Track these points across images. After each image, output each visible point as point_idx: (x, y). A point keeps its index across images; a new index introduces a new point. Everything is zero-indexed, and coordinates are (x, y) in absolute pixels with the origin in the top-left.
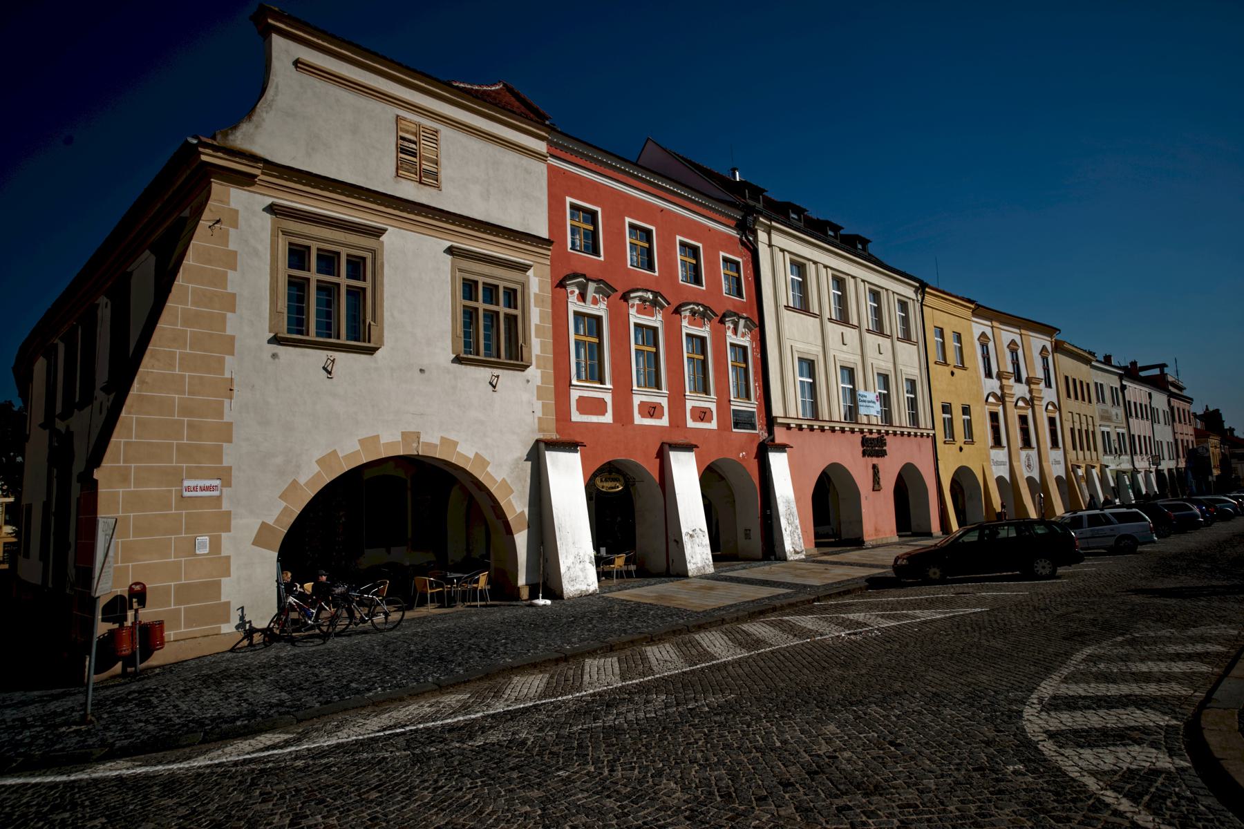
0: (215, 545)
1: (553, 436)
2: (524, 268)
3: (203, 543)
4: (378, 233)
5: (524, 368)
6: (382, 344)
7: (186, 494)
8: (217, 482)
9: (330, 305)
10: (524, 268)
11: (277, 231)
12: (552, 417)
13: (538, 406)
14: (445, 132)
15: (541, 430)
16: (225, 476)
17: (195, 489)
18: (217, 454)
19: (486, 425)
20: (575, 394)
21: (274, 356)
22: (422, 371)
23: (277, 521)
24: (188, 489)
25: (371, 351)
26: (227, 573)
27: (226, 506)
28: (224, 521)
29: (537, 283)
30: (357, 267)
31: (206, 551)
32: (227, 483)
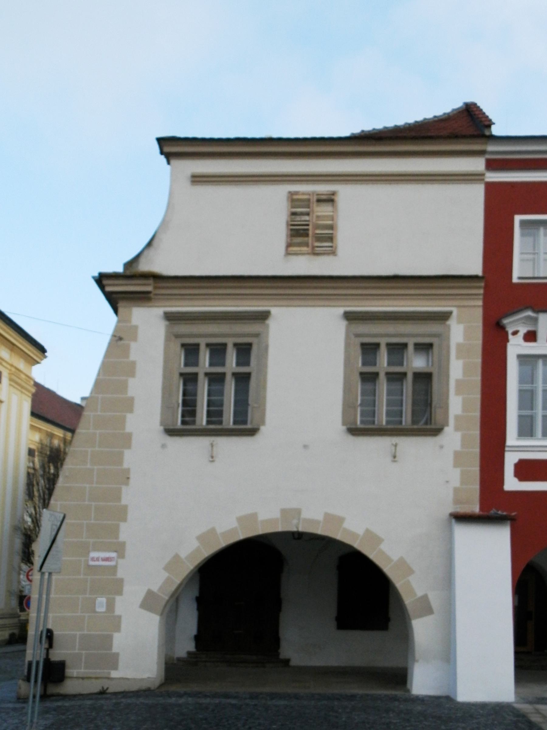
0: (111, 605)
1: (476, 509)
2: (444, 317)
3: (101, 603)
4: (264, 316)
5: (436, 431)
6: (263, 422)
7: (91, 563)
8: (113, 555)
9: (216, 394)
10: (444, 317)
11: (171, 336)
12: (475, 487)
13: (455, 477)
14: (345, 193)
15: (457, 501)
16: (120, 549)
17: (98, 559)
18: (115, 531)
19: (397, 502)
20: (510, 460)
21: (164, 446)
22: (305, 447)
23: (161, 588)
24: (93, 559)
25: (252, 432)
26: (118, 629)
27: (120, 574)
28: (117, 587)
29: (463, 331)
30: (244, 351)
31: (103, 609)
32: (121, 555)
